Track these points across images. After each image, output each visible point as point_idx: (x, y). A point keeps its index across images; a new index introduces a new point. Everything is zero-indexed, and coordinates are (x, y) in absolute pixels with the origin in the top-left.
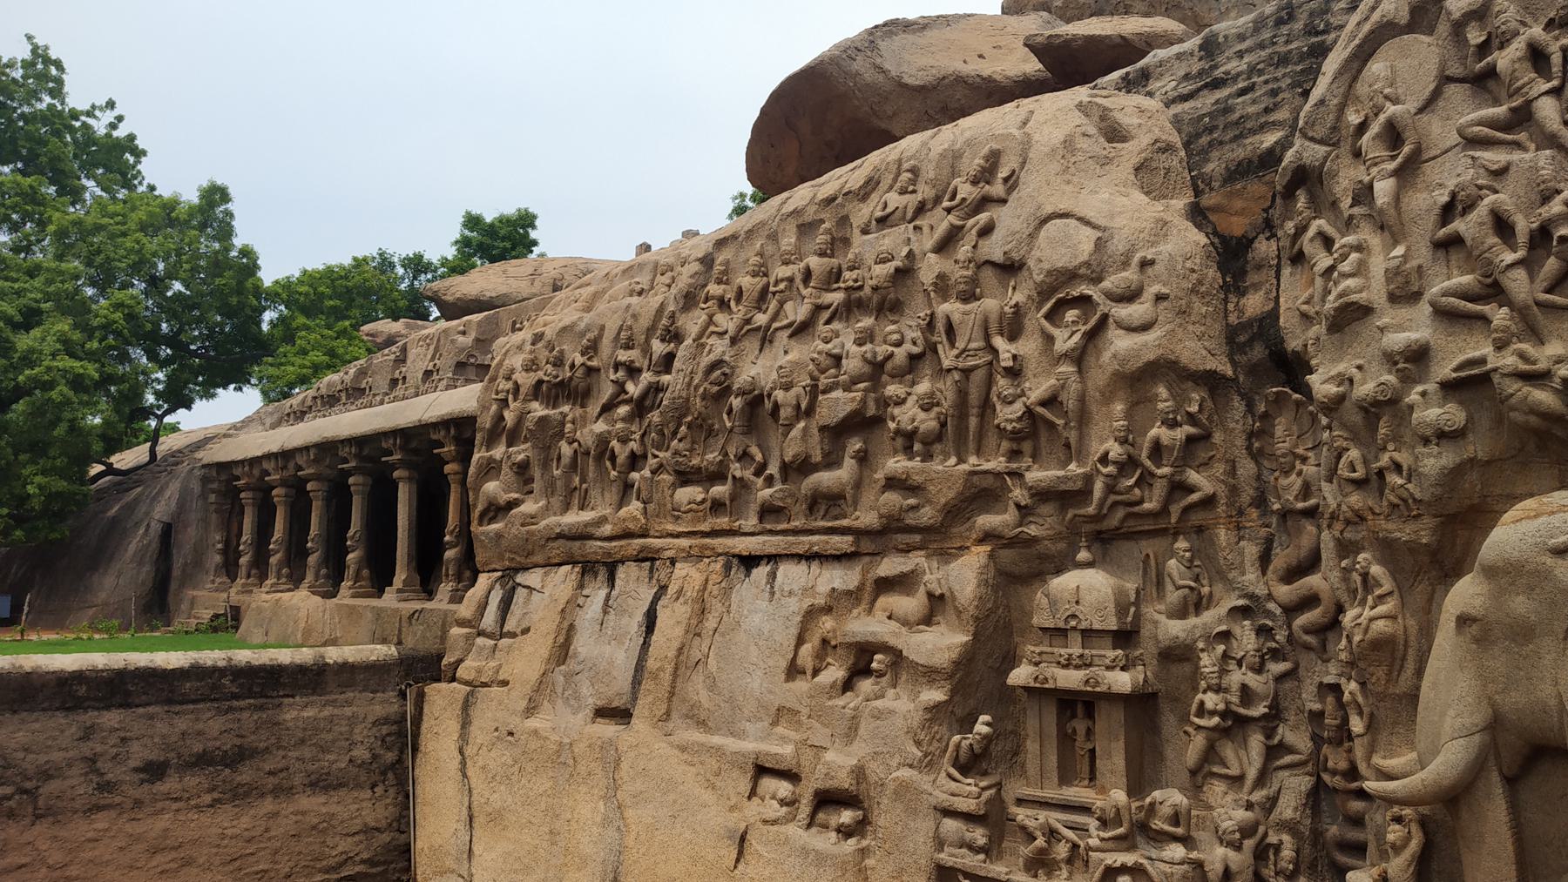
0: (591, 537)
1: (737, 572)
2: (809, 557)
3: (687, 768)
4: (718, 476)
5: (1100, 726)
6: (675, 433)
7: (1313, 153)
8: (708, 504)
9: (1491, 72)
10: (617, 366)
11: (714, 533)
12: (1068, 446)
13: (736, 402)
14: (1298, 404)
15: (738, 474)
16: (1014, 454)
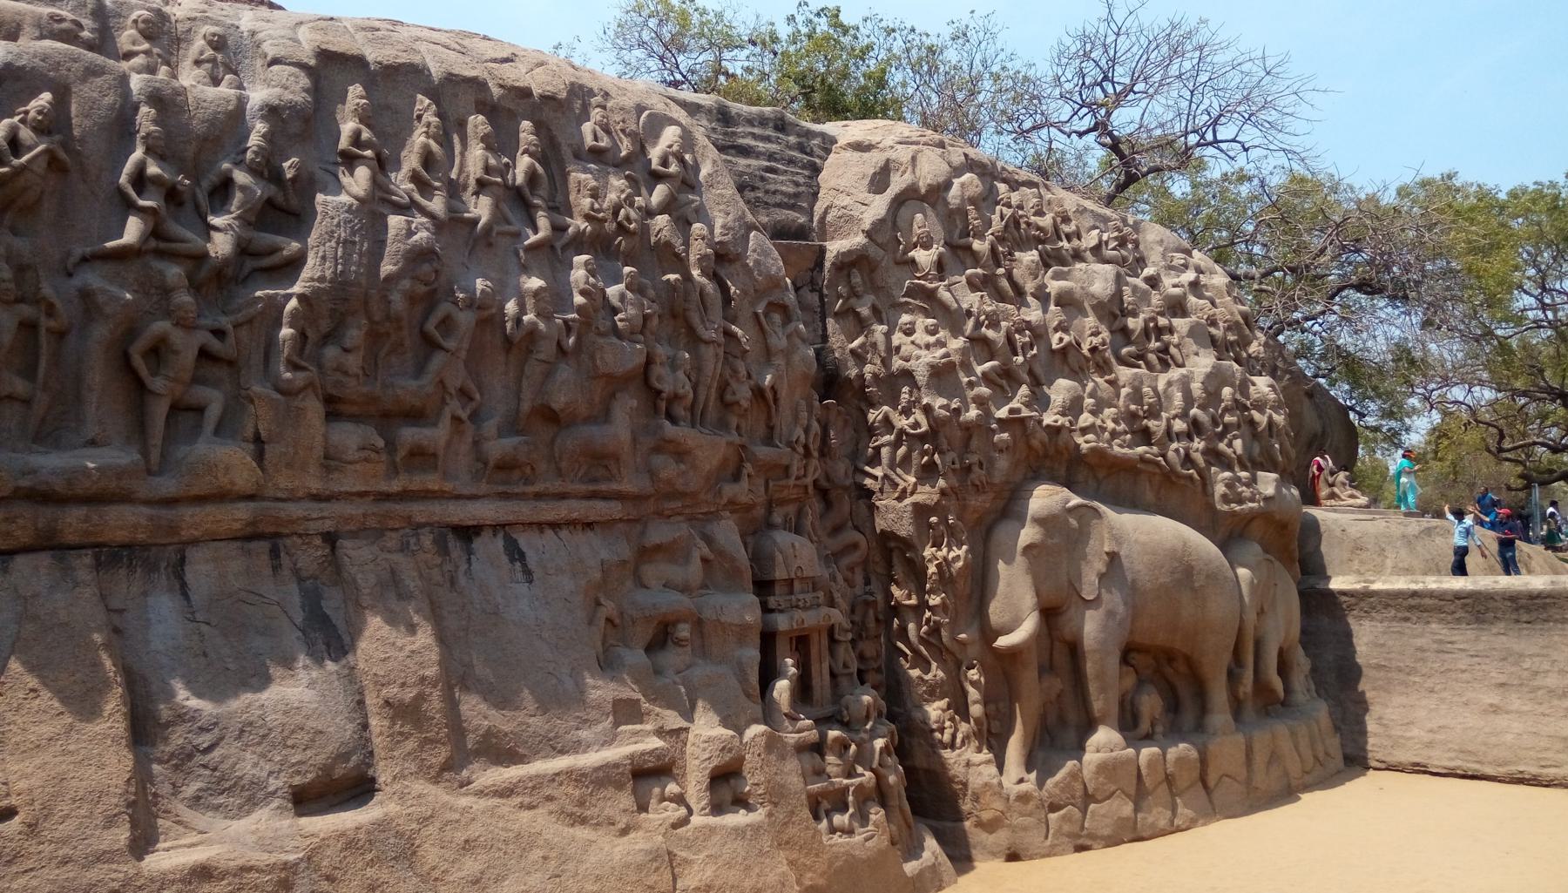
0: (125, 498)
1: (454, 545)
2: (555, 526)
3: (532, 813)
4: (415, 416)
5: (814, 651)
6: (327, 339)
7: (874, 252)
8: (402, 453)
9: (969, 248)
10: (140, 180)
11: (405, 496)
12: (771, 428)
13: (465, 319)
14: (839, 413)
15: (464, 415)
16: (738, 428)
